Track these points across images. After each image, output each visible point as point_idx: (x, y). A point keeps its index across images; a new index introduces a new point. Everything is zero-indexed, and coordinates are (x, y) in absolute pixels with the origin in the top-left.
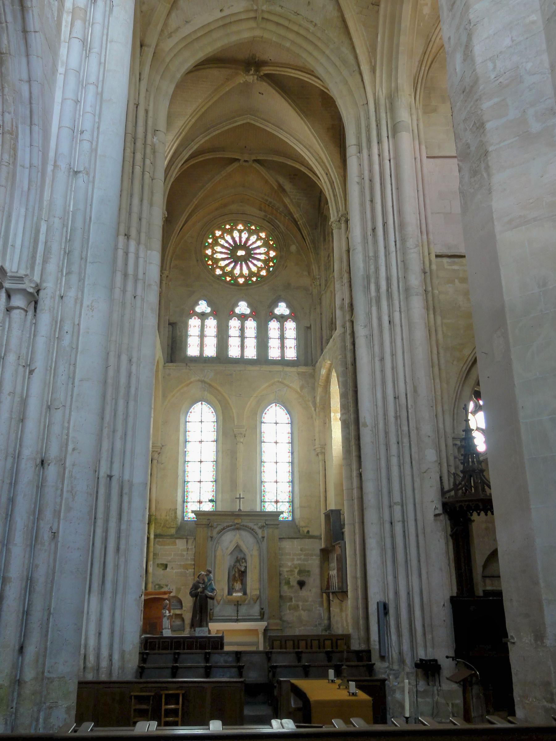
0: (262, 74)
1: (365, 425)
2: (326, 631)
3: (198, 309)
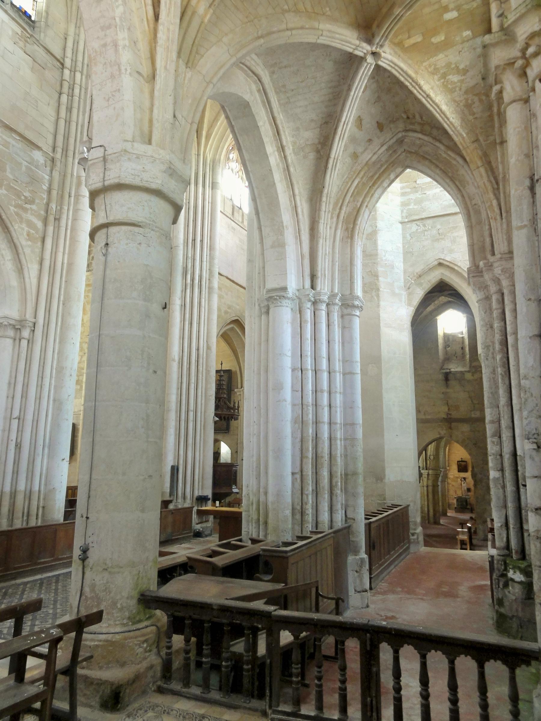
1: (174, 360)
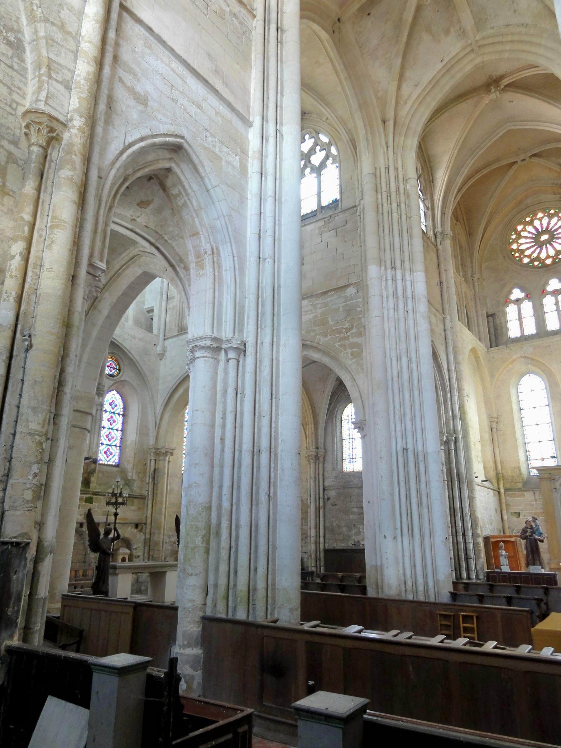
0: (502, 87)
3: (513, 297)
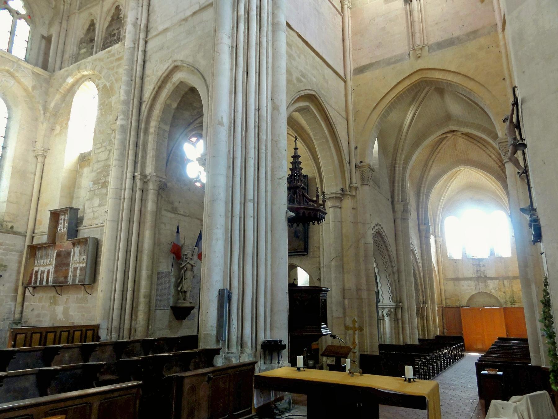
1: (221, 124)
2: (17, 325)
